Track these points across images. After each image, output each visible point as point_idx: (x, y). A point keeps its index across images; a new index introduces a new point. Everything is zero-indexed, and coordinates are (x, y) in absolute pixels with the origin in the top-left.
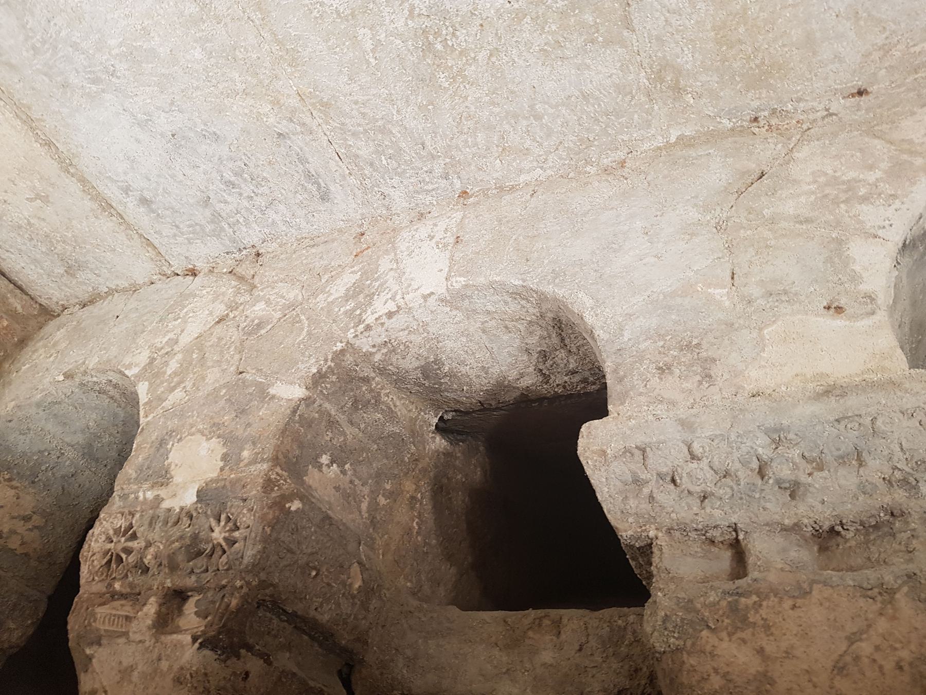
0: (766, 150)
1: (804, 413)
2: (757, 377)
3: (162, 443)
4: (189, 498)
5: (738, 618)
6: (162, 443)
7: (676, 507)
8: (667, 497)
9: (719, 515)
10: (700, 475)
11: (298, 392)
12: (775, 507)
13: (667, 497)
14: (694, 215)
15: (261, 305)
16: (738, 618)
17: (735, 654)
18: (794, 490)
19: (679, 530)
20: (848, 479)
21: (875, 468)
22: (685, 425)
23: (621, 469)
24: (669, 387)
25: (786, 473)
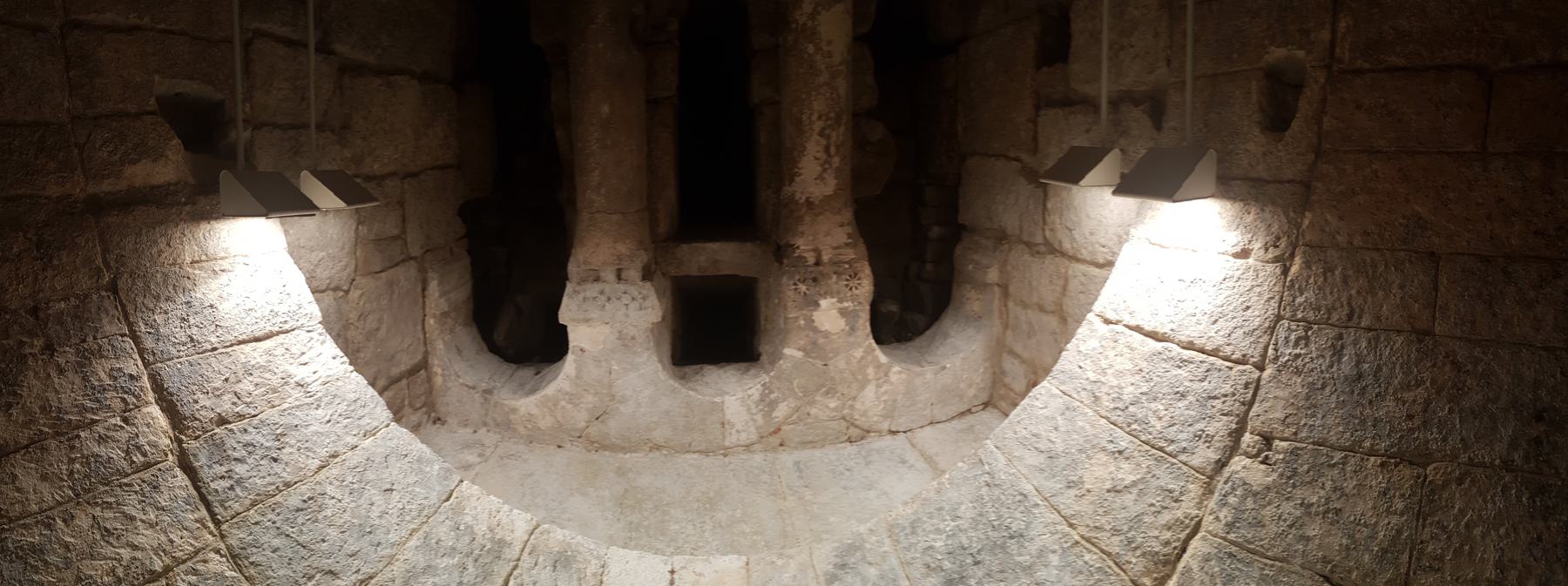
0: (595, 430)
1: (595, 314)
2: (606, 329)
3: (853, 329)
4: (824, 303)
5: (620, 257)
6: (853, 329)
7: (633, 290)
8: (636, 294)
9: (622, 287)
10: (626, 299)
11: (787, 351)
12: (607, 288)
13: (636, 294)
14: (622, 408)
15: (832, 405)
16: (620, 257)
17: (622, 248)
18: (602, 293)
19: (633, 284)
20: (588, 294)
21: (581, 296)
22: (627, 316)
23: (648, 303)
24: (632, 331)
25: (604, 298)
